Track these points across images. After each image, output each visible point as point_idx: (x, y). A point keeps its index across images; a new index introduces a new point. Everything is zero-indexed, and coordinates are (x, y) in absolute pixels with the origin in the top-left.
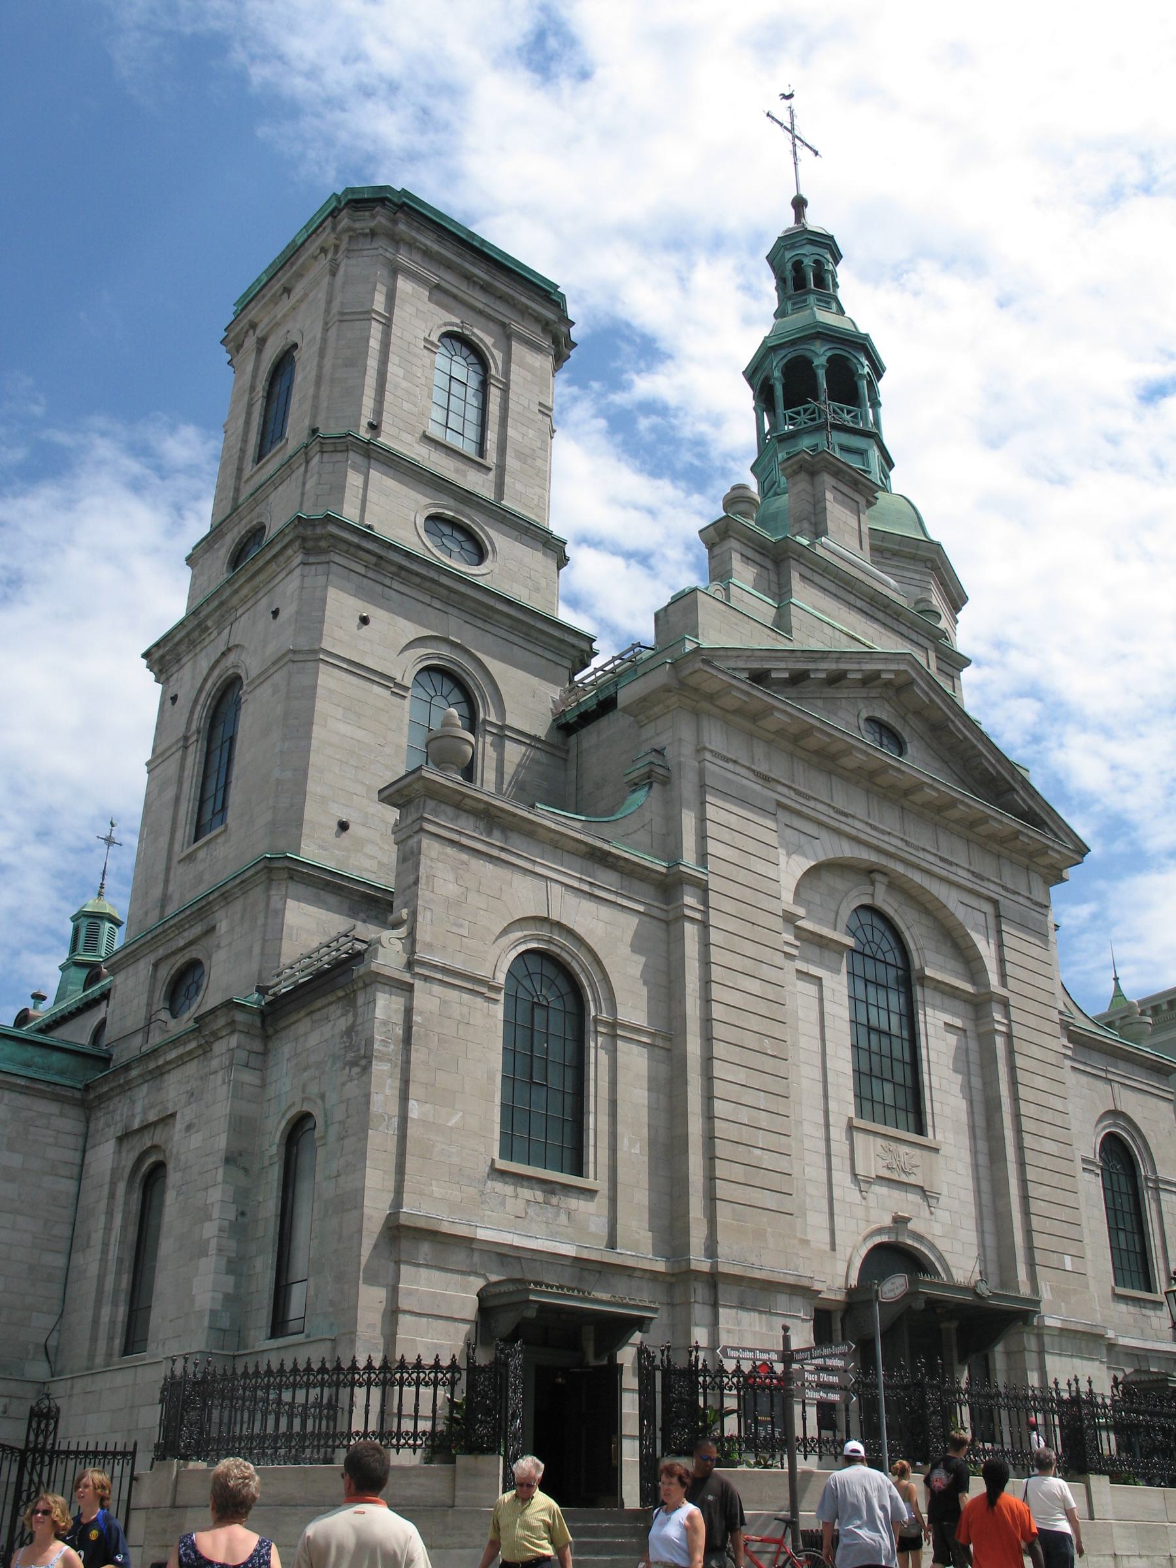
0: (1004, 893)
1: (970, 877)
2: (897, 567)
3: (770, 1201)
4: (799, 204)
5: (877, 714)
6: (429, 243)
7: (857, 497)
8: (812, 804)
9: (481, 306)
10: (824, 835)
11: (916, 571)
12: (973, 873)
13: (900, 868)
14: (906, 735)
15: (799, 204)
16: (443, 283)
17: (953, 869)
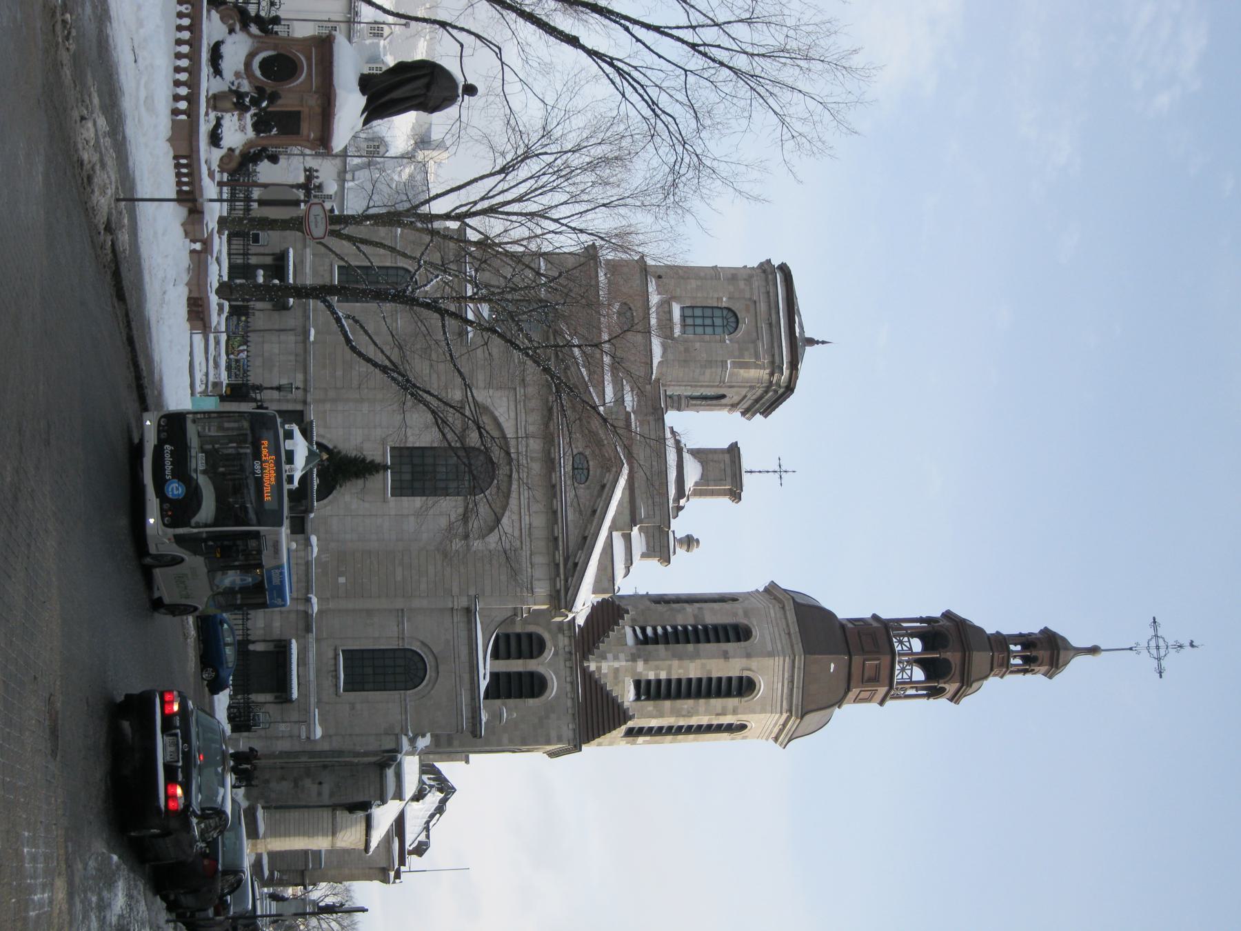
0: (528, 555)
1: (528, 526)
2: (780, 635)
3: (339, 373)
4: (1094, 650)
5: (591, 463)
6: (771, 291)
7: (729, 480)
8: (523, 411)
9: (759, 325)
10: (513, 422)
11: (783, 647)
12: (530, 528)
13: (515, 475)
14: (587, 483)
15: (1094, 650)
16: (758, 304)
17: (527, 513)
